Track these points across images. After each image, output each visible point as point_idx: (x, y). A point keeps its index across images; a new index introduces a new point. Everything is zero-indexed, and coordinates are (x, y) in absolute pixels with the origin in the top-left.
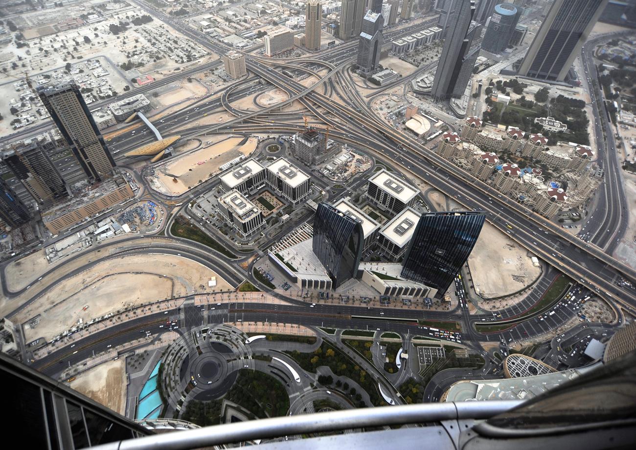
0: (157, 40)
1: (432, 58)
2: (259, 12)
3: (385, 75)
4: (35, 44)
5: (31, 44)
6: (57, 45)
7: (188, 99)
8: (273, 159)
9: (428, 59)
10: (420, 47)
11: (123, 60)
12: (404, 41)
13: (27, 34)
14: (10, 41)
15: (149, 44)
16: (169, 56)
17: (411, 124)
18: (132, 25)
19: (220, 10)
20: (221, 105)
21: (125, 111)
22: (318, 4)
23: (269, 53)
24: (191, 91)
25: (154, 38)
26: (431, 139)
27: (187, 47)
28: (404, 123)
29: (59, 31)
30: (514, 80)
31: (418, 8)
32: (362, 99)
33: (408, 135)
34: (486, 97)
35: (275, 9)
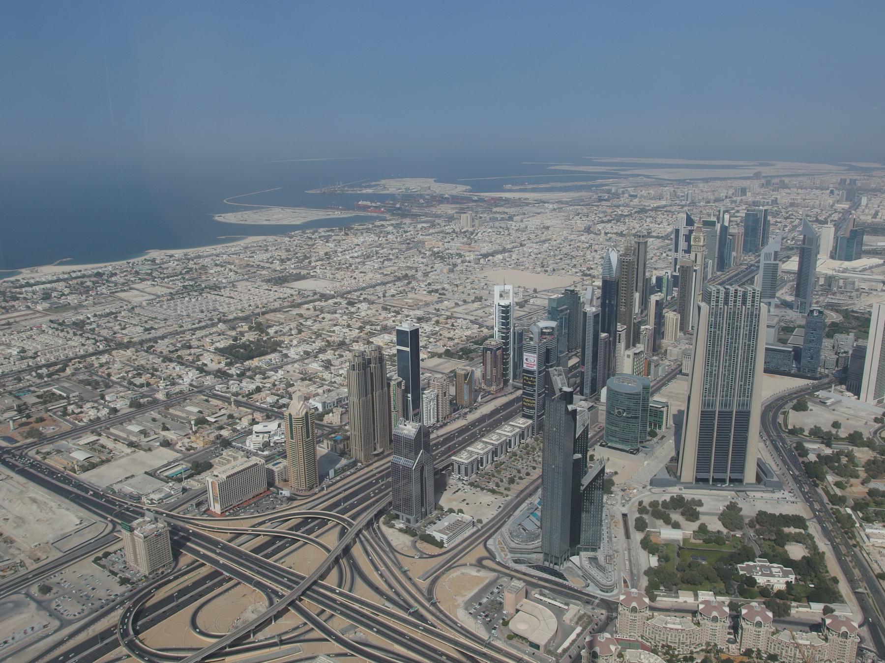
1: (528, 474)
2: (193, 422)
3: (449, 528)
9: (521, 478)
10: (502, 458)
12: (471, 453)
17: (518, 625)
20: (115, 645)
22: (307, 413)
23: (217, 508)
26: (565, 651)
28: (506, 623)
31: (483, 385)
32: (415, 585)
33: (519, 649)
35: (223, 411)
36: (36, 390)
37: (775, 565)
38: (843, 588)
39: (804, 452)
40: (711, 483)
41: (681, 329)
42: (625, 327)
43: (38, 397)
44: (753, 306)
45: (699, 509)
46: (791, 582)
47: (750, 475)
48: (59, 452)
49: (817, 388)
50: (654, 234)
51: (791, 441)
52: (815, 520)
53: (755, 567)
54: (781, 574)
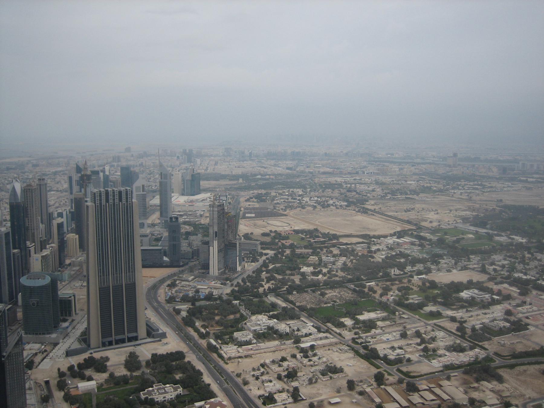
30: (89, 357)
34: (62, 393)
37: (168, 385)
38: (215, 387)
39: (178, 312)
40: (114, 343)
41: (80, 248)
42: (34, 244)
44: (127, 201)
45: (108, 364)
46: (180, 394)
47: (142, 331)
49: (182, 272)
50: (55, 189)
51: (169, 307)
52: (191, 352)
53: (153, 390)
54: (172, 390)
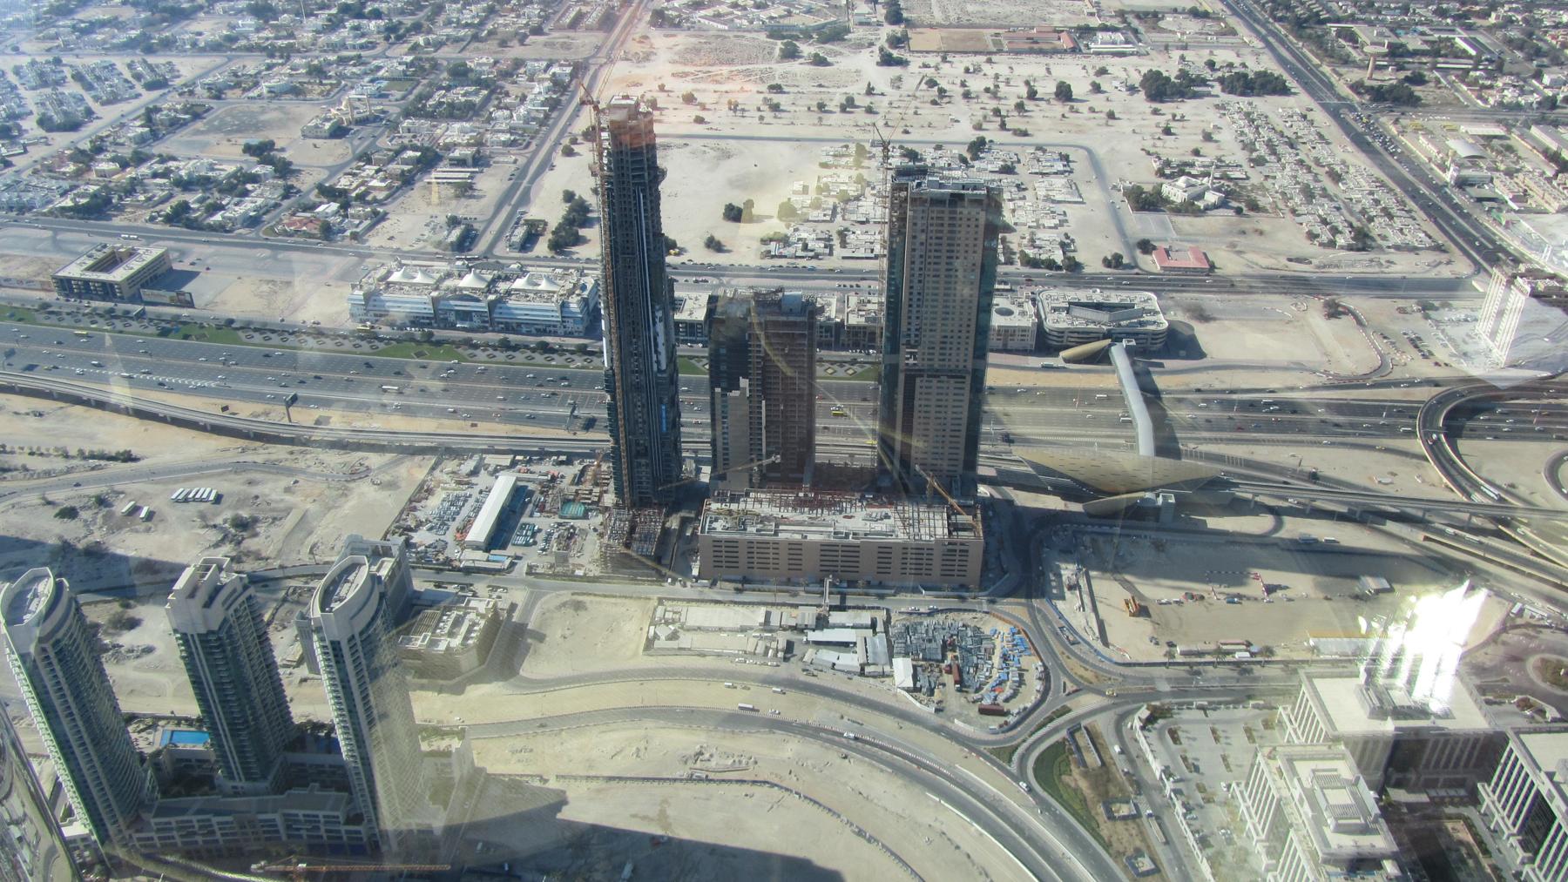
0: (1274, 152)
4: (926, 66)
5: (916, 62)
6: (976, 84)
7: (1300, 367)
8: (1542, 712)
11: (1144, 175)
13: (918, 39)
14: (871, 44)
15: (1241, 157)
16: (1293, 211)
18: (1217, 89)
19: (1541, 121)
21: (1079, 324)
24: (1319, 342)
25: (1270, 145)
27: (1367, 202)
29: (1000, 51)
36: (1428, 31)
43: (1426, 42)
48: (1428, 133)
